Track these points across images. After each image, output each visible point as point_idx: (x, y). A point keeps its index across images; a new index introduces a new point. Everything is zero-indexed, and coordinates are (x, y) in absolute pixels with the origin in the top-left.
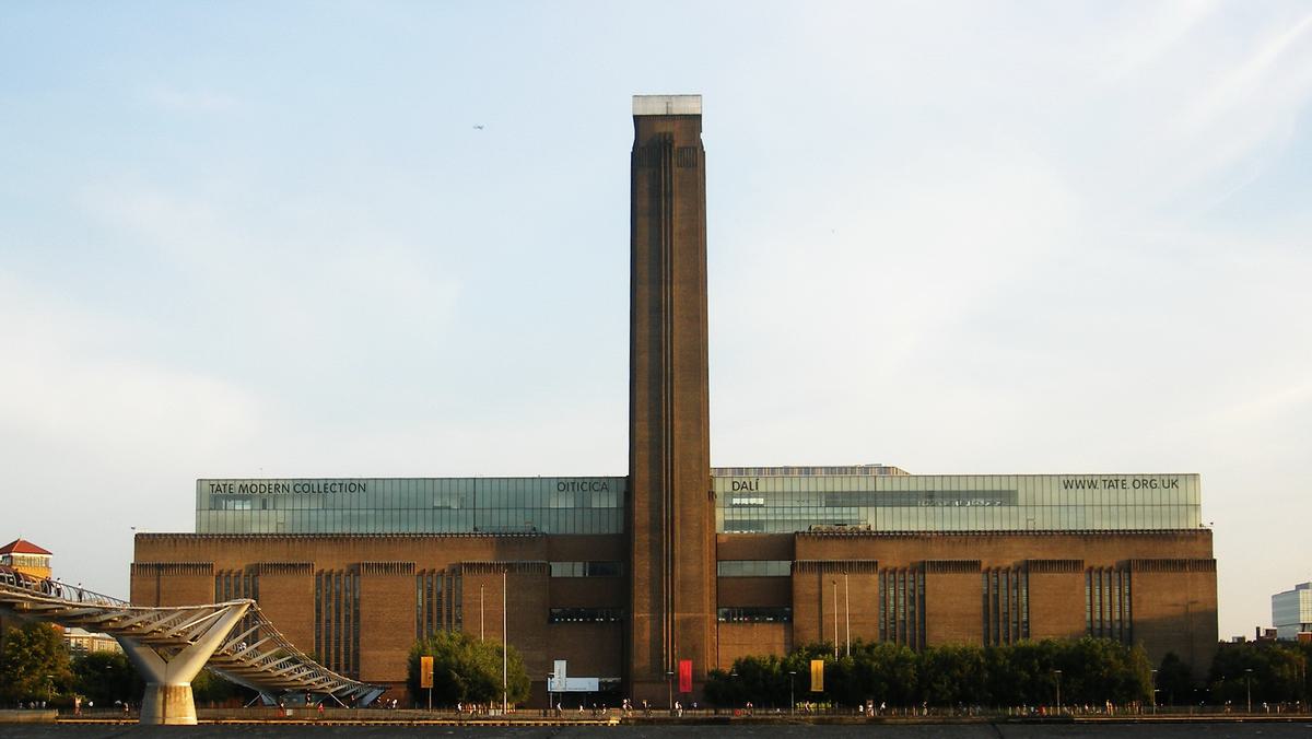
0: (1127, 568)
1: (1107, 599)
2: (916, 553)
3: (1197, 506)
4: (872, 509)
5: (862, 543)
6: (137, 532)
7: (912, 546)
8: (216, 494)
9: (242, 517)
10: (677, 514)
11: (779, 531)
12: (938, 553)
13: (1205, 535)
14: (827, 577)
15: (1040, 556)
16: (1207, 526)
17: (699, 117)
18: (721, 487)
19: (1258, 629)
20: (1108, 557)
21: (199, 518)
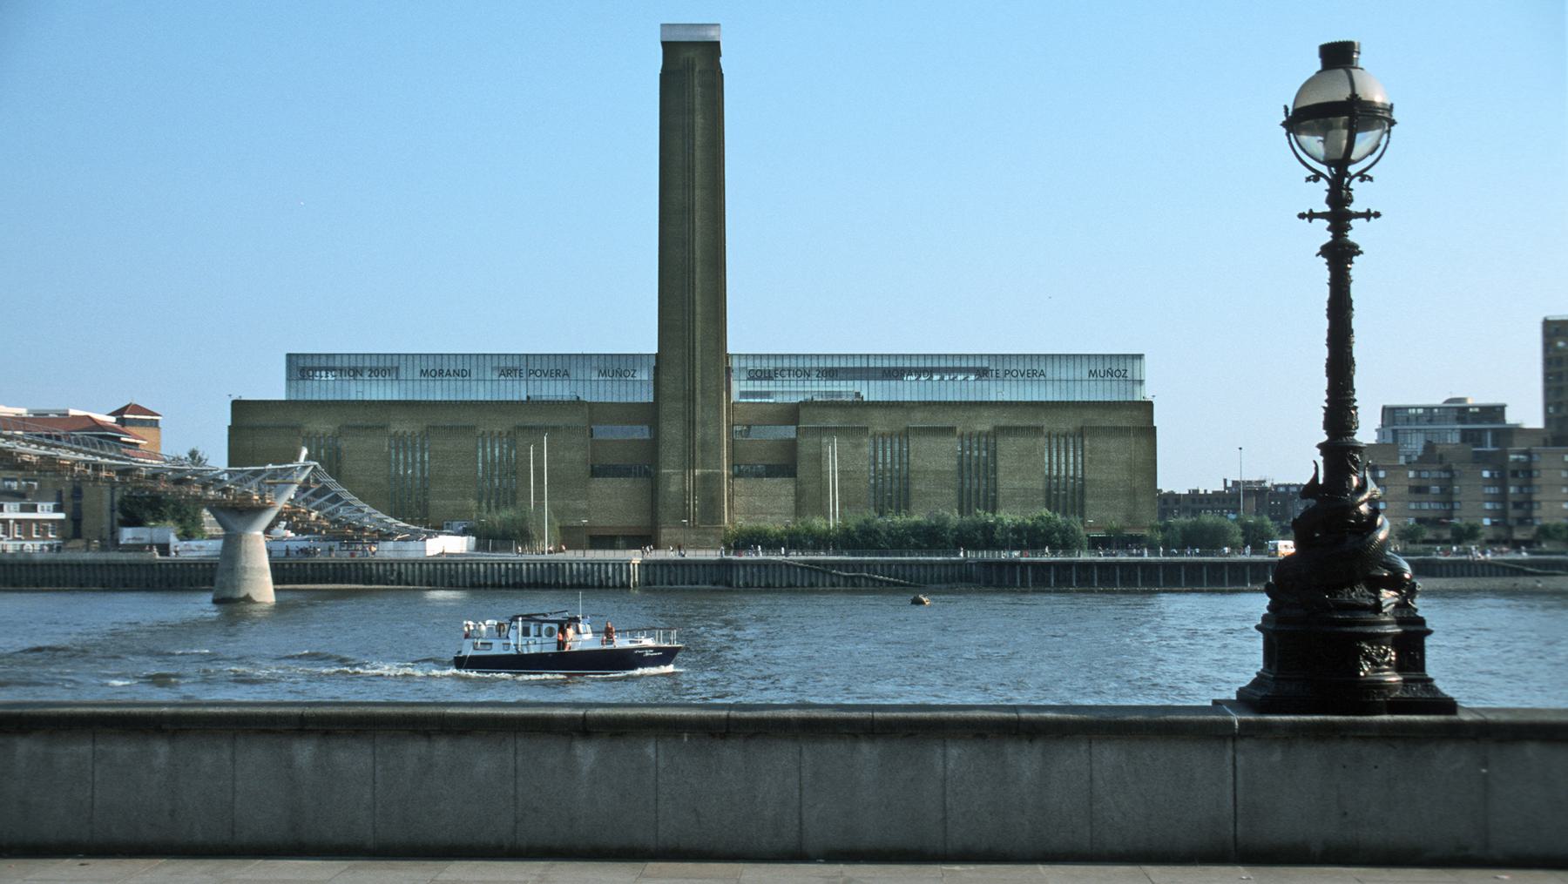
0: (1081, 433)
1: (1071, 460)
2: (900, 421)
3: (1141, 382)
4: (865, 382)
5: (855, 411)
6: (235, 397)
7: (896, 415)
8: (300, 367)
9: (324, 388)
10: (698, 386)
11: (787, 399)
12: (918, 419)
13: (1148, 406)
14: (825, 440)
15: (1003, 422)
16: (1149, 398)
17: (718, 43)
18: (735, 364)
19: (1225, 481)
20: (1068, 423)
21: (289, 387)
